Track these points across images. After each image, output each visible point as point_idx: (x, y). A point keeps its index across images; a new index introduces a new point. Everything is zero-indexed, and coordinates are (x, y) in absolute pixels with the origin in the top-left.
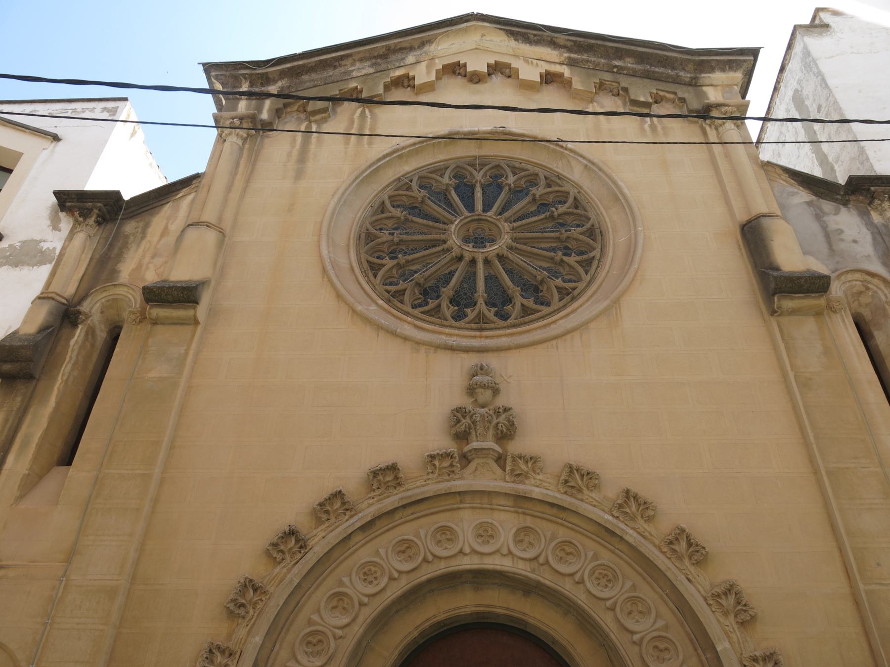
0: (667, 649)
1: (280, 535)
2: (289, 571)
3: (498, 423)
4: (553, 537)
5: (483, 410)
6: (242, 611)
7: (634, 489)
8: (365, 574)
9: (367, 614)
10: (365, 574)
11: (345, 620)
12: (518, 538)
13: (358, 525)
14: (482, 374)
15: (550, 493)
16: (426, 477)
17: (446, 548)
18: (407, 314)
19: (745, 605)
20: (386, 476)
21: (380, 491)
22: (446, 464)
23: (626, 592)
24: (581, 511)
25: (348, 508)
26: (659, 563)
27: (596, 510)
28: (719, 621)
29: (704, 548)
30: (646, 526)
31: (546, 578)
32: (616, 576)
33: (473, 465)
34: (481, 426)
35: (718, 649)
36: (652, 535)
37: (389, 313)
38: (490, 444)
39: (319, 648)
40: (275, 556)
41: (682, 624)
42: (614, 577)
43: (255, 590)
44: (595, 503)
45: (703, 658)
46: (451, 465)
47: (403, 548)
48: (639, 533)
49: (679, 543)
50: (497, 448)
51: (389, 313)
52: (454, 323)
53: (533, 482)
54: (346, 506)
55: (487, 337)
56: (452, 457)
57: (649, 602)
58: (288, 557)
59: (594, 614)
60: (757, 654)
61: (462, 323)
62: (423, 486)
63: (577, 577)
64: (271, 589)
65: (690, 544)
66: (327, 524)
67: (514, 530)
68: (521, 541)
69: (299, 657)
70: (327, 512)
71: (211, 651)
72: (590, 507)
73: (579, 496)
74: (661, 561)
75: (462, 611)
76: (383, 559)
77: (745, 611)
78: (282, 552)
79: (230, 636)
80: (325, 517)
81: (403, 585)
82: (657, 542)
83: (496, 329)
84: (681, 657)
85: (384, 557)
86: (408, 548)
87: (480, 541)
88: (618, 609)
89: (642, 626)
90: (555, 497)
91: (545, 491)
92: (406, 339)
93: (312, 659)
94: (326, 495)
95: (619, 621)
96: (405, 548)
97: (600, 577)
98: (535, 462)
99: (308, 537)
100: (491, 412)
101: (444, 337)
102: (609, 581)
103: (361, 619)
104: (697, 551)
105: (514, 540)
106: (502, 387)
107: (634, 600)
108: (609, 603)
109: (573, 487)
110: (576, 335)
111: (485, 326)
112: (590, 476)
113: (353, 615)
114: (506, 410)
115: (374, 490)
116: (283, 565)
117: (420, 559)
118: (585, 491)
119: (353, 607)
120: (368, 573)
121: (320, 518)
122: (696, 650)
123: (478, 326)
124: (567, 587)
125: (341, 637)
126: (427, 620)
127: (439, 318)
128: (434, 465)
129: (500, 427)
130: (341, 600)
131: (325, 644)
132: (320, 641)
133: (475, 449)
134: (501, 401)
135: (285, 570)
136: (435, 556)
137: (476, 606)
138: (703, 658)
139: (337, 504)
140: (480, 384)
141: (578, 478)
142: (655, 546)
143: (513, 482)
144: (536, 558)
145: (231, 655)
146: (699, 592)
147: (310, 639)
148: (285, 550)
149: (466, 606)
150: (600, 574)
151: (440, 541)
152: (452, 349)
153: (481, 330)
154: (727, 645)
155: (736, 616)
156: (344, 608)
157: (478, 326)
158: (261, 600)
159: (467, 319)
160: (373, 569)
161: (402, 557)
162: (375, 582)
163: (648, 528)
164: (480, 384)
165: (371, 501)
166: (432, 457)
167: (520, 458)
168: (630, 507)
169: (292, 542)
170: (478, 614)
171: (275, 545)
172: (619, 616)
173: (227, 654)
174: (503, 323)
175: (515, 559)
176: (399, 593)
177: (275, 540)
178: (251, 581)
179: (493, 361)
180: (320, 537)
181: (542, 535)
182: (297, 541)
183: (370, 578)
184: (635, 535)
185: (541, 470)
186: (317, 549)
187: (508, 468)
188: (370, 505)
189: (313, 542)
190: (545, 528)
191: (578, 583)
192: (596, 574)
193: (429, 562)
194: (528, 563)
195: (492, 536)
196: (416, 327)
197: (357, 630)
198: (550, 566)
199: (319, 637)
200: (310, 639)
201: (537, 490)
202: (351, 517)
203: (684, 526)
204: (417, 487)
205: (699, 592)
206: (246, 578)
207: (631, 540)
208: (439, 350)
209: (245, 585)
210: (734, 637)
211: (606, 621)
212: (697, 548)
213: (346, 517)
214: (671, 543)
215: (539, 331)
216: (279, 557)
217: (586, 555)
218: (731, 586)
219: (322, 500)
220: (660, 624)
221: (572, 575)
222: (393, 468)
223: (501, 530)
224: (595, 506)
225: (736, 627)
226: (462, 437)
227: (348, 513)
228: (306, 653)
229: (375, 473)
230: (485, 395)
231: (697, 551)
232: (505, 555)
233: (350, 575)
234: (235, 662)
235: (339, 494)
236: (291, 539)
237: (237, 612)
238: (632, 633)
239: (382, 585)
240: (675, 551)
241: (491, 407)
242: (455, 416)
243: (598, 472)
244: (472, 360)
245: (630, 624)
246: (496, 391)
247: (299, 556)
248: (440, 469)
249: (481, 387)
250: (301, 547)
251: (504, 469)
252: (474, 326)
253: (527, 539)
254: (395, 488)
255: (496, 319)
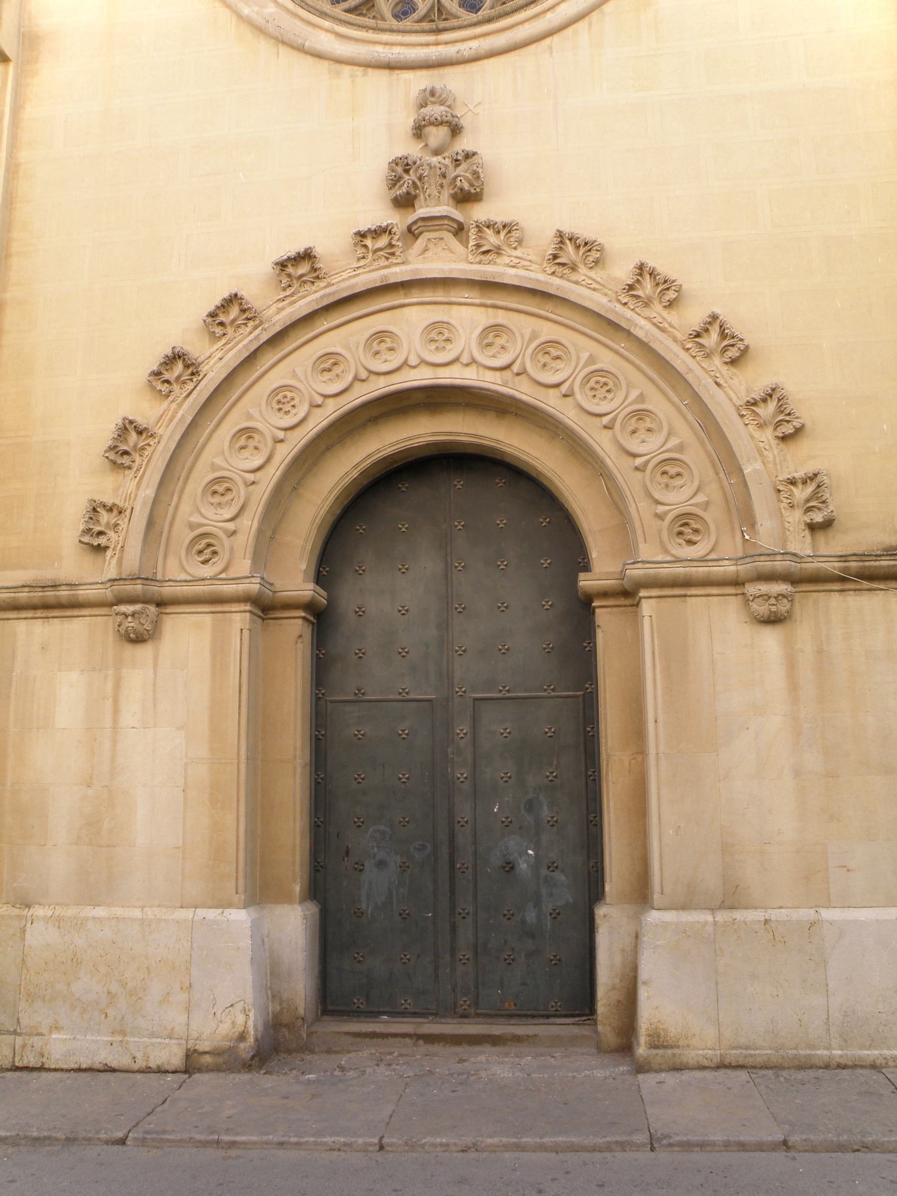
0: (679, 474)
1: (162, 360)
2: (180, 405)
3: (456, 177)
4: (534, 335)
5: (435, 160)
6: (126, 460)
7: (651, 263)
8: (279, 402)
9: (285, 453)
10: (279, 402)
11: (257, 462)
12: (486, 341)
13: (265, 337)
14: (434, 103)
15: (532, 275)
16: (356, 265)
17: (386, 361)
18: (323, 15)
19: (789, 414)
20: (299, 265)
21: (292, 289)
22: (383, 241)
23: (630, 404)
24: (573, 298)
25: (249, 314)
26: (677, 364)
27: (596, 296)
28: (752, 437)
29: (741, 340)
30: (665, 313)
31: (523, 391)
32: (618, 385)
33: (420, 243)
34: (439, 184)
35: (745, 472)
36: (673, 327)
37: (296, 15)
38: (445, 208)
39: (229, 497)
40: (158, 388)
41: (702, 443)
42: (615, 385)
43: (140, 433)
44: (594, 285)
45: (726, 484)
46: (391, 245)
47: (327, 365)
48: (655, 324)
49: (709, 336)
50: (457, 214)
51: (296, 15)
52: (394, 23)
53: (506, 260)
54: (247, 315)
55: (446, 43)
56: (390, 233)
57: (661, 416)
58: (176, 387)
59: (585, 435)
60: (797, 475)
61: (407, 23)
62: (355, 276)
63: (564, 388)
64: (160, 431)
65: (723, 335)
66: (223, 341)
67: (480, 329)
68: (489, 345)
69: (203, 510)
70: (221, 324)
71: (94, 510)
72: (587, 292)
73: (574, 277)
74: (680, 359)
75: (415, 443)
76: (301, 381)
77: (788, 422)
78: (167, 381)
79: (116, 490)
80: (219, 330)
81: (331, 411)
82: (679, 336)
83: (460, 28)
84: (696, 484)
85: (302, 378)
86: (335, 364)
87: (433, 346)
88: (617, 426)
89: (648, 446)
90: (538, 280)
91: (522, 272)
92: (319, 56)
93: (221, 511)
94: (218, 301)
95: (618, 442)
96: (329, 363)
97: (598, 386)
98: (509, 232)
99: (200, 360)
100: (447, 161)
101: (379, 48)
102: (608, 391)
103: (277, 460)
104: (733, 345)
105: (480, 344)
106: (463, 122)
107: (640, 414)
108: (605, 420)
109: (564, 265)
110: (582, 25)
111: (442, 24)
112: (587, 248)
113: (267, 455)
114: (468, 156)
115: (284, 289)
116: (171, 399)
117: (350, 378)
118: (583, 269)
119: (266, 445)
120: (281, 398)
121: (214, 332)
122: (717, 474)
123: (433, 26)
124: (551, 402)
125: (253, 483)
126: (369, 456)
127: (374, 17)
128: (365, 246)
129: (458, 183)
130: (250, 437)
131: (234, 492)
132: (228, 490)
133: (424, 219)
134: (464, 144)
135: (174, 405)
136: (371, 372)
137: (433, 434)
138: (726, 484)
139: (234, 311)
140: (438, 122)
141: (574, 250)
142: (675, 340)
143: (480, 263)
144: (508, 367)
145: (120, 513)
146: (731, 400)
147: (216, 487)
148: (172, 380)
149: (419, 436)
150: (597, 382)
151: (377, 353)
152: (391, 66)
153: (439, 31)
154: (758, 465)
155: (775, 429)
156: (256, 448)
157: (433, 26)
158: (149, 445)
159: (416, 16)
160: (289, 394)
161: (327, 376)
162: (293, 411)
163: (672, 317)
164: (438, 122)
165: (281, 305)
166: (362, 235)
167: (488, 227)
168: (643, 289)
169: (179, 367)
170: (436, 444)
171: (157, 374)
172: (619, 437)
173: (115, 512)
174: (472, 17)
175: (481, 370)
176: (325, 423)
177: (155, 368)
178: (131, 422)
179: (452, 81)
180: (216, 358)
181: (517, 335)
182: (187, 366)
183: (287, 407)
184: (648, 326)
185: (520, 242)
186: (211, 375)
187: (472, 243)
188: (280, 310)
189: (205, 368)
190: (522, 325)
191: (565, 396)
192: (592, 383)
193: (363, 381)
194: (498, 374)
195: (448, 340)
196: (339, 35)
197: (273, 473)
198: (528, 375)
199: (227, 485)
200: (216, 487)
201: (513, 271)
202: (256, 328)
203: (718, 311)
204: (344, 280)
205: (731, 400)
206: (124, 419)
207: (640, 334)
208: (370, 70)
209: (126, 428)
210: (770, 455)
211: (602, 442)
212: (731, 341)
213: (248, 330)
214: (698, 335)
215: (526, 25)
216: (165, 388)
217: (578, 358)
218: (773, 390)
219: (212, 308)
220: (674, 442)
221: (557, 386)
222: (307, 256)
223: (461, 331)
224: (594, 290)
225: (774, 442)
226: (404, 202)
227: (251, 324)
228: (212, 504)
229: (282, 265)
230: (437, 135)
231: (733, 345)
232: (467, 365)
233: (260, 405)
234: (126, 520)
235: (233, 299)
236: (176, 366)
237: (119, 462)
238: (635, 456)
239: (301, 415)
240: (701, 346)
241: (446, 154)
242: (393, 171)
243: (600, 240)
244: (420, 81)
245: (633, 445)
246: (456, 130)
247: (190, 386)
248: (375, 251)
249: (431, 124)
250: (193, 374)
251: (467, 247)
252: (425, 25)
253: (499, 341)
254: (313, 283)
255: (461, 12)
